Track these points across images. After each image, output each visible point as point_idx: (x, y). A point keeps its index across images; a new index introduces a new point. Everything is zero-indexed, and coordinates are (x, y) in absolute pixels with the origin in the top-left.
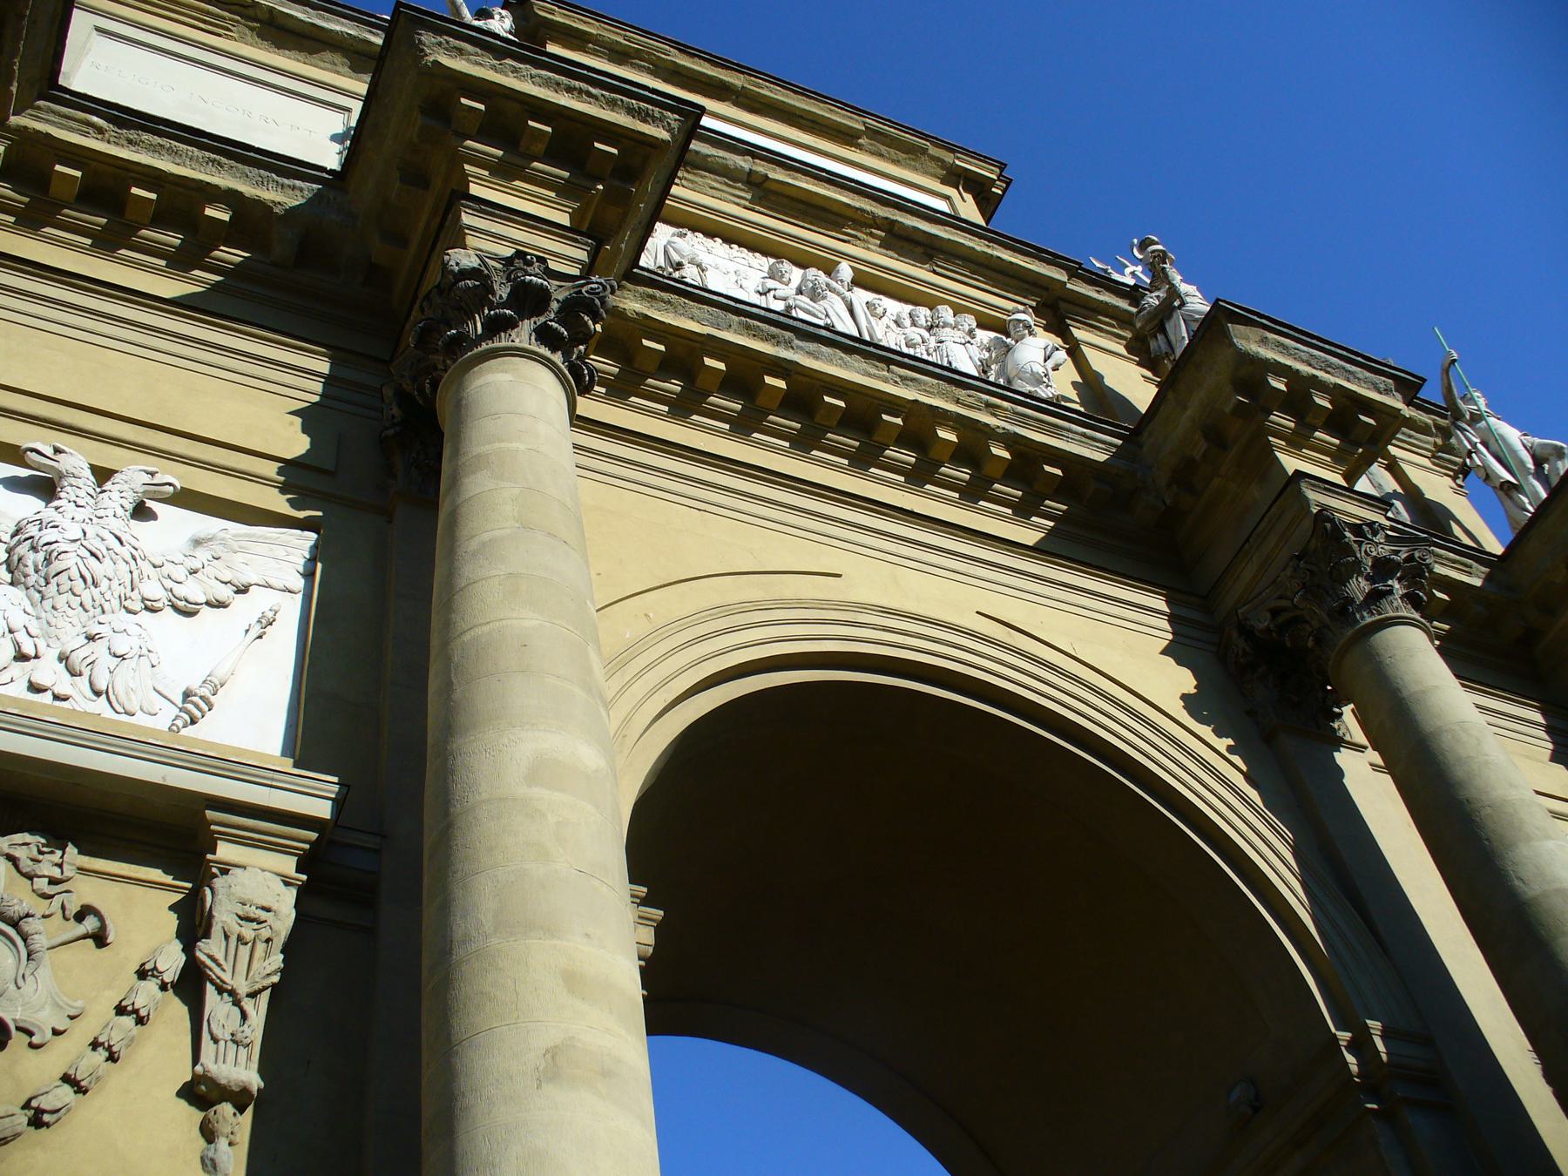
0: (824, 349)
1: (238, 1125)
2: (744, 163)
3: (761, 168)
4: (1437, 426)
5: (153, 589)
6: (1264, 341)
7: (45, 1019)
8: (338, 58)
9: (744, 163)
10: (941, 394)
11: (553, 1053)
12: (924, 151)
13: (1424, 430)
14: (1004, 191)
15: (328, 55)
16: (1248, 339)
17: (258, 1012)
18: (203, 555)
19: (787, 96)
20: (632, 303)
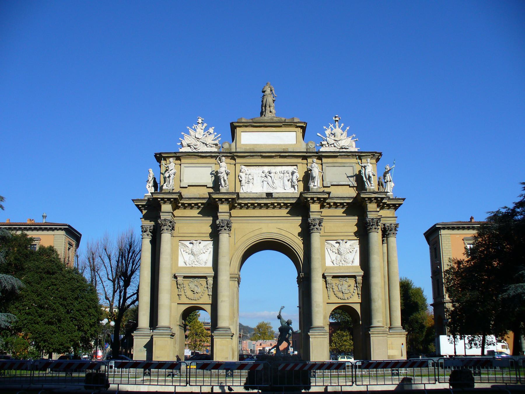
0: (261, 199)
1: (211, 296)
2: (259, 154)
3: (261, 154)
4: (371, 154)
5: (202, 252)
6: (307, 194)
7: (200, 291)
8: (209, 157)
9: (259, 154)
10: (275, 200)
11: (222, 301)
12: (292, 125)
13: (370, 155)
14: (306, 126)
15: (208, 157)
16: (305, 195)
17: (211, 289)
18: (204, 247)
19: (270, 124)
20: (240, 201)
